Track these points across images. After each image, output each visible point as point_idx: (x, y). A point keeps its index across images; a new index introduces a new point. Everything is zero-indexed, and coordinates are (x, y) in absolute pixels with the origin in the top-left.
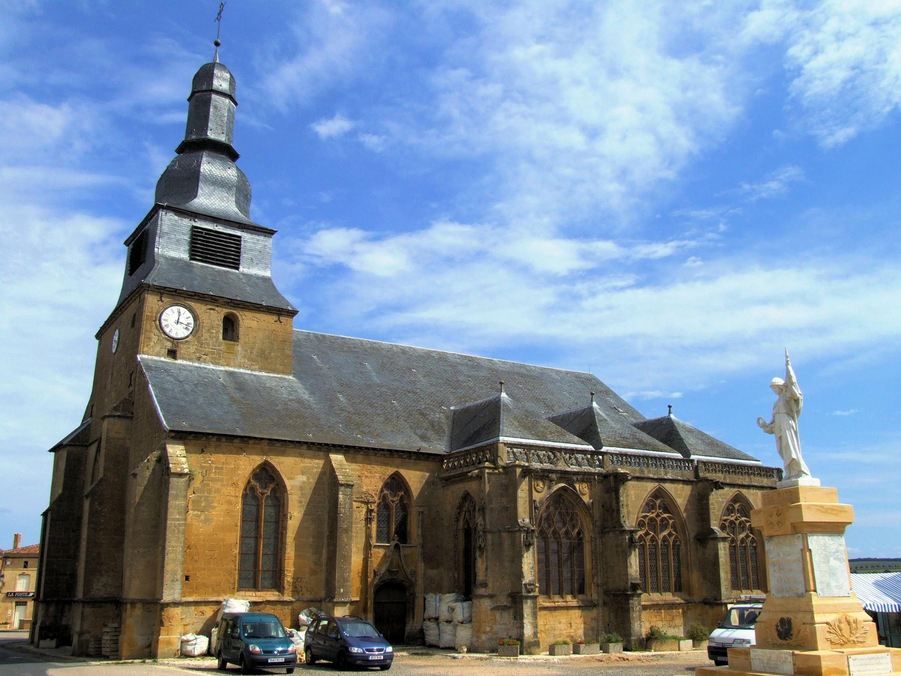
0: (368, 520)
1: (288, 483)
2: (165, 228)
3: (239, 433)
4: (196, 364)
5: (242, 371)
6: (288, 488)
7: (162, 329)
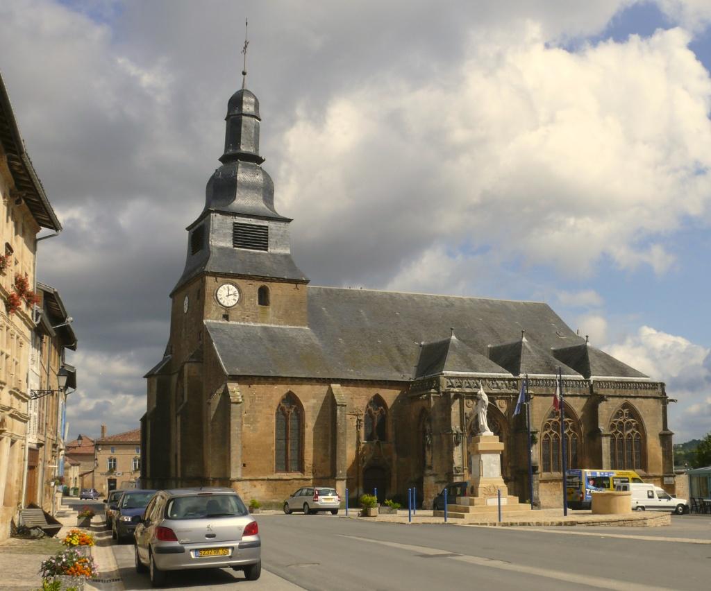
0: (358, 427)
2: (216, 226)
3: (272, 374)
4: (242, 324)
5: (273, 326)
6: (305, 408)
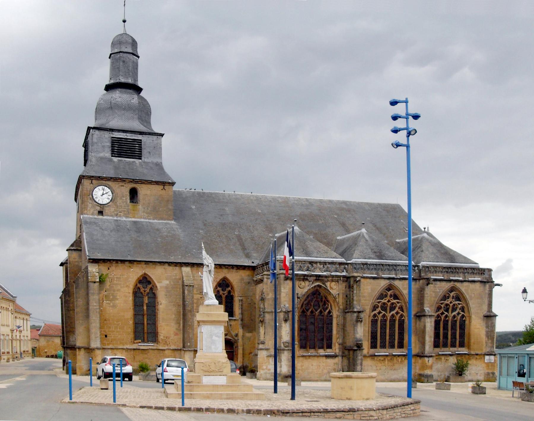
1: (158, 285)
3: (129, 258)
4: (115, 218)
5: (142, 220)
6: (159, 287)
7: (94, 200)
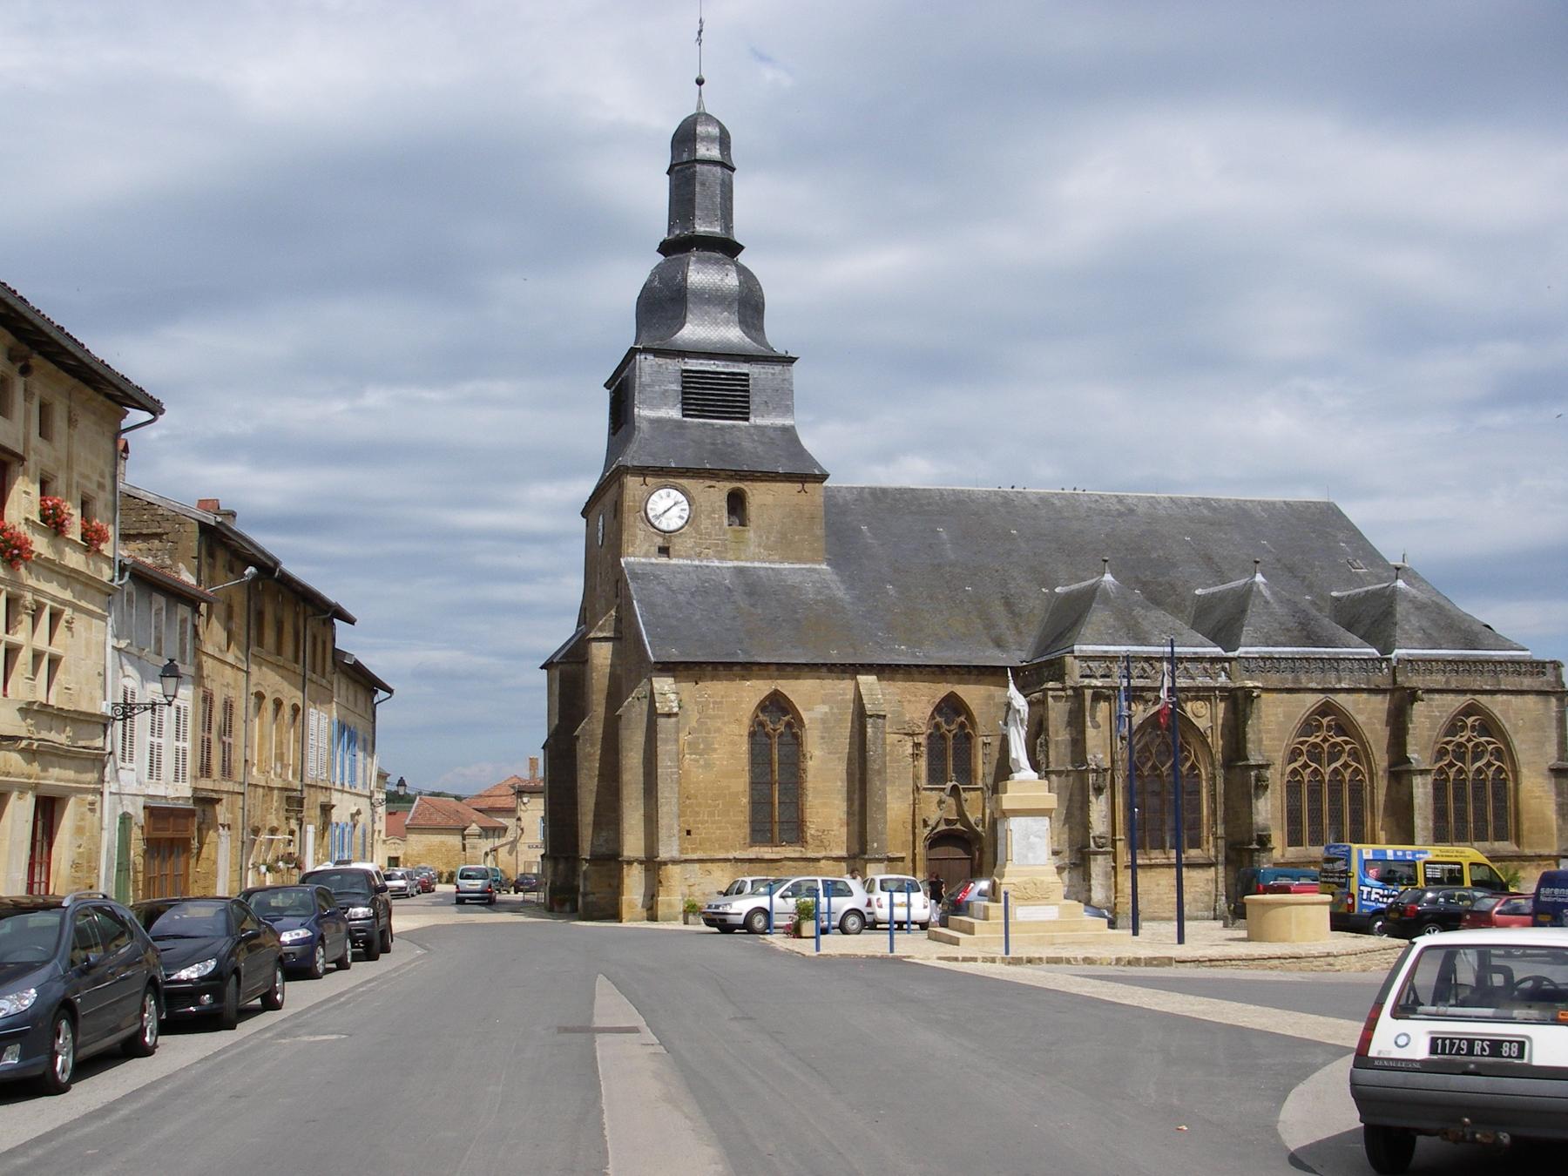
0: (915, 756)
2: (646, 379)
3: (742, 658)
4: (697, 563)
5: (757, 564)
